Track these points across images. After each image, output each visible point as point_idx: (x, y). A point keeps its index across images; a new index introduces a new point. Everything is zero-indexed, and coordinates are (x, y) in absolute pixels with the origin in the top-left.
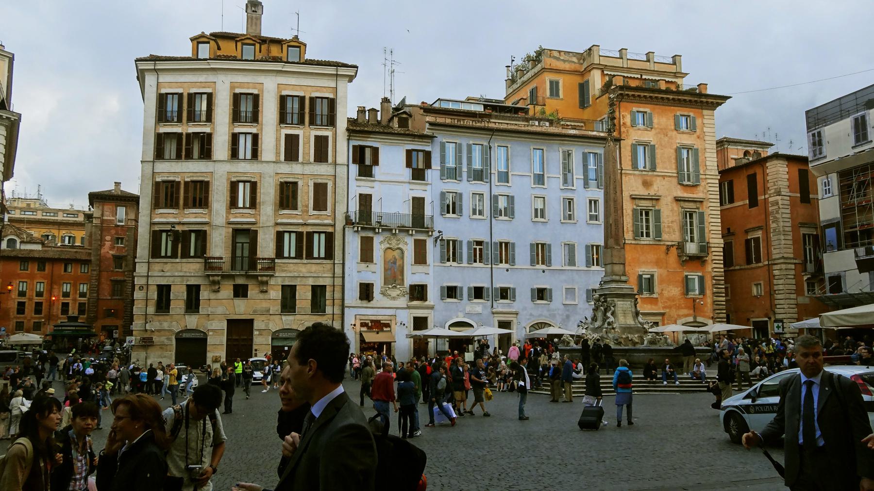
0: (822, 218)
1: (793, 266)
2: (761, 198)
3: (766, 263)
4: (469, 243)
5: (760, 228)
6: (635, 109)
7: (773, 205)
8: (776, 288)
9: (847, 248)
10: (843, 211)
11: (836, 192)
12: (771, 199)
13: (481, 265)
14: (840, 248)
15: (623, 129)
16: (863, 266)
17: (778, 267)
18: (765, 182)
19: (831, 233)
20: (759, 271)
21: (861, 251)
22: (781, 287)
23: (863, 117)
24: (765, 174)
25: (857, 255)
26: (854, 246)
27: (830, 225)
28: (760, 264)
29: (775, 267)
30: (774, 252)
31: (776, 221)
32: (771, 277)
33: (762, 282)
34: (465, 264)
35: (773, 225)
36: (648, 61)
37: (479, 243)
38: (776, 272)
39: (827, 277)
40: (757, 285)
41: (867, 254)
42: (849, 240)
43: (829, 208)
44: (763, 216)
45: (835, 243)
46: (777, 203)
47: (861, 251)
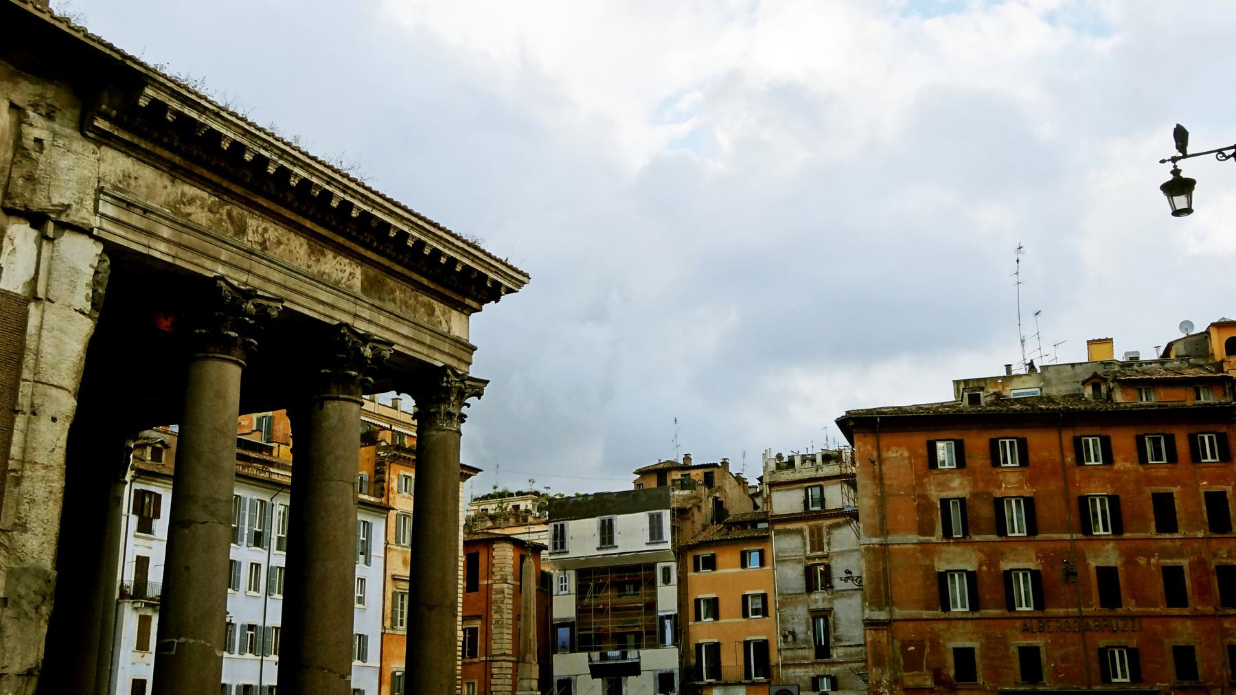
0: (555, 616)
1: (511, 665)
2: (483, 582)
3: (484, 658)
4: (242, 626)
5: (479, 617)
6: (402, 473)
7: (497, 593)
8: (493, 688)
9: (581, 650)
10: (579, 611)
11: (573, 590)
12: (495, 586)
13: (251, 656)
14: (572, 651)
15: (391, 495)
16: (596, 671)
17: (498, 664)
18: (490, 565)
19: (564, 633)
20: (473, 668)
21: (596, 656)
22: (499, 688)
23: (610, 521)
24: (490, 557)
25: (590, 659)
26: (589, 650)
27: (564, 624)
28: (476, 660)
29: (494, 664)
30: (495, 646)
31: (500, 611)
32: (488, 675)
33: (476, 681)
34: (236, 655)
35: (496, 616)
36: (395, 408)
37: (251, 627)
38: (494, 671)
39: (555, 680)
40: (468, 684)
41: (601, 659)
42: (580, 643)
43: (564, 607)
44: (483, 605)
45: (568, 644)
46: (503, 592)
47: (596, 656)
